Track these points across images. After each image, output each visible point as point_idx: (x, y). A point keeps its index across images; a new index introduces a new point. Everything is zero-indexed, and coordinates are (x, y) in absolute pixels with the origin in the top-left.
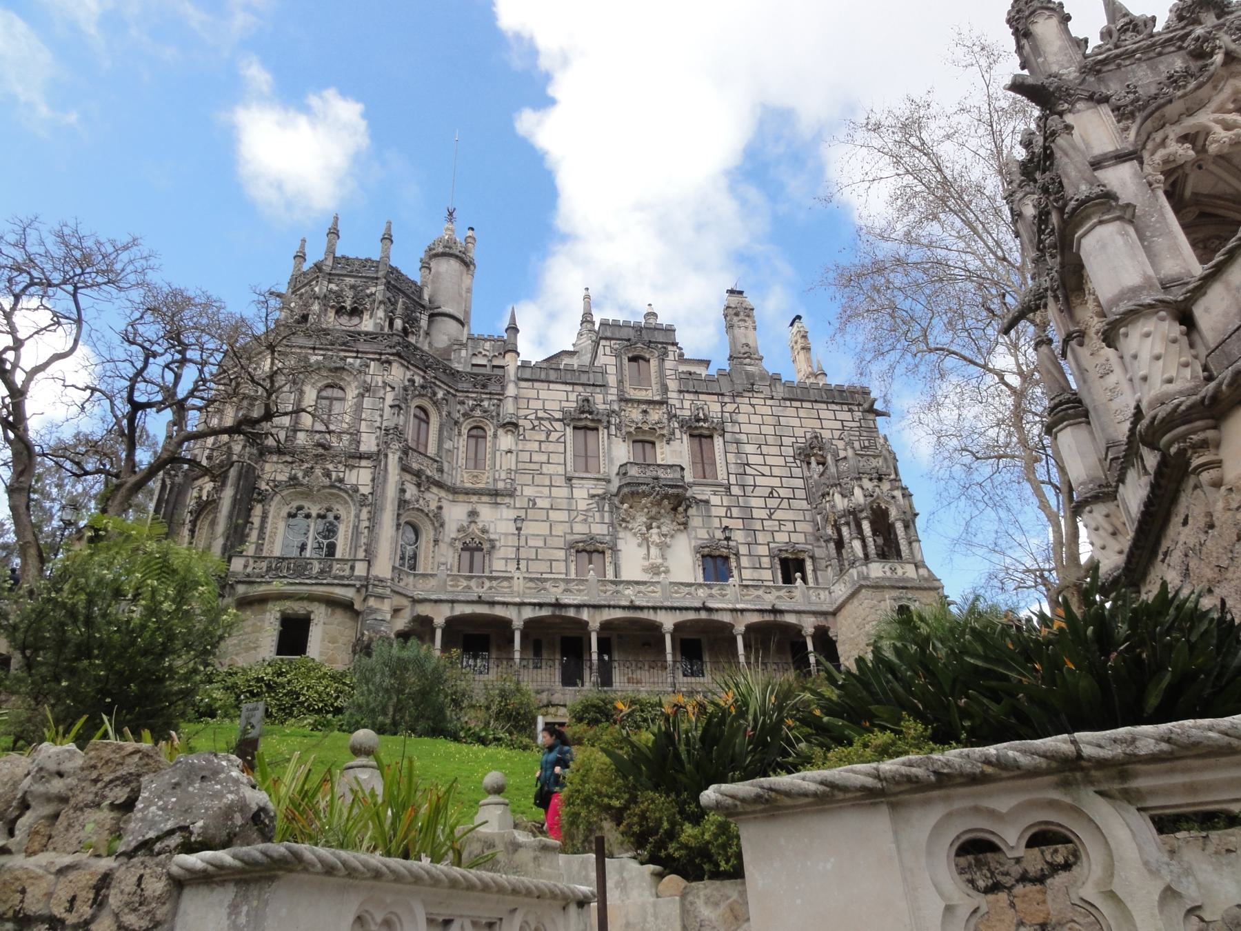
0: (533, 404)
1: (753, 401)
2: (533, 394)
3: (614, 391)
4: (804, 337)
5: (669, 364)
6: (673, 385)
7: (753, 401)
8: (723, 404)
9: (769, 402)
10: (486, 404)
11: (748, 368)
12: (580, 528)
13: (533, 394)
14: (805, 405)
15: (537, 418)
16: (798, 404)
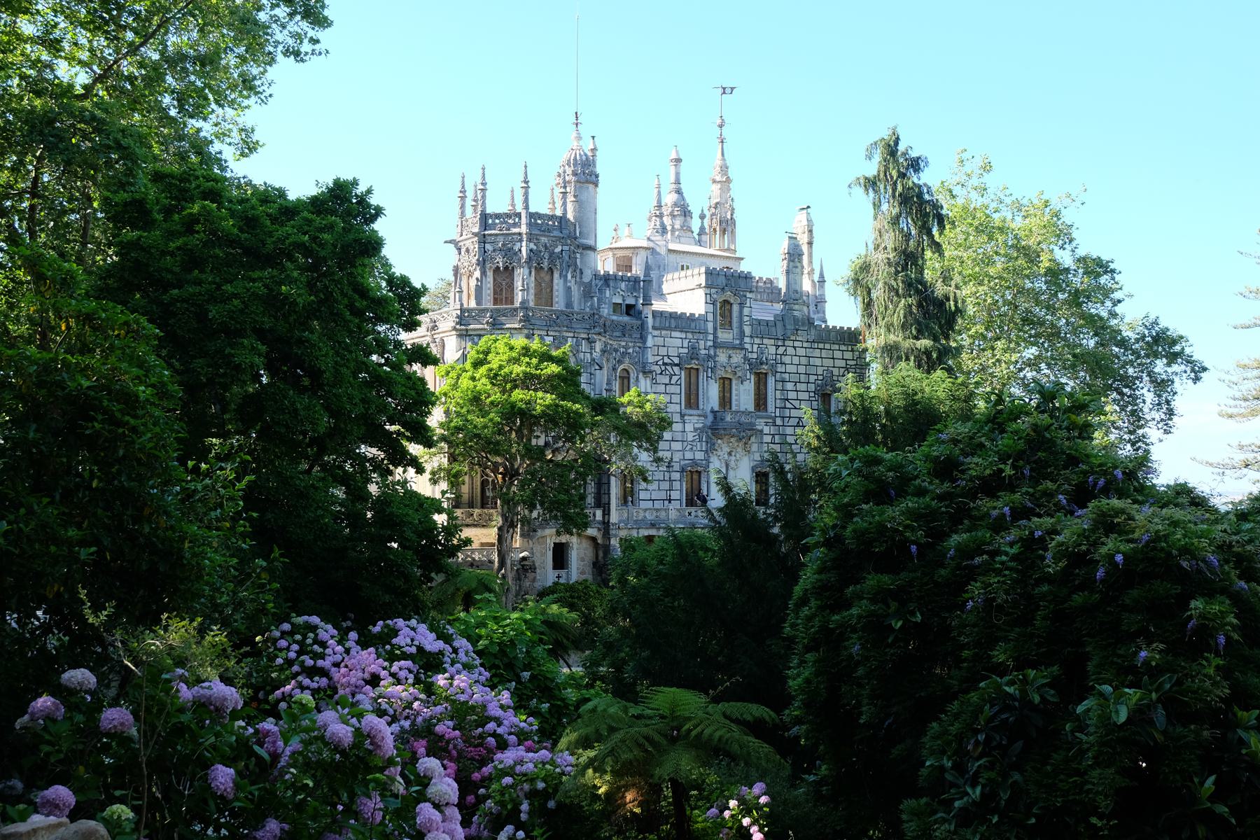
0: (663, 351)
1: (796, 344)
2: (660, 341)
3: (711, 337)
4: (810, 231)
5: (746, 311)
6: (747, 330)
7: (796, 344)
8: (777, 347)
9: (805, 345)
10: (631, 351)
11: (796, 313)
12: (689, 455)
13: (660, 341)
14: (827, 346)
15: (665, 364)
16: (821, 346)
